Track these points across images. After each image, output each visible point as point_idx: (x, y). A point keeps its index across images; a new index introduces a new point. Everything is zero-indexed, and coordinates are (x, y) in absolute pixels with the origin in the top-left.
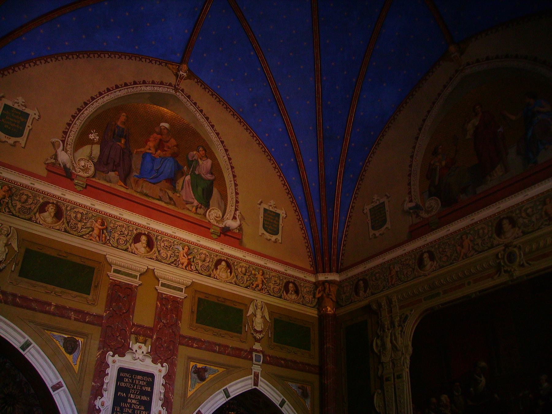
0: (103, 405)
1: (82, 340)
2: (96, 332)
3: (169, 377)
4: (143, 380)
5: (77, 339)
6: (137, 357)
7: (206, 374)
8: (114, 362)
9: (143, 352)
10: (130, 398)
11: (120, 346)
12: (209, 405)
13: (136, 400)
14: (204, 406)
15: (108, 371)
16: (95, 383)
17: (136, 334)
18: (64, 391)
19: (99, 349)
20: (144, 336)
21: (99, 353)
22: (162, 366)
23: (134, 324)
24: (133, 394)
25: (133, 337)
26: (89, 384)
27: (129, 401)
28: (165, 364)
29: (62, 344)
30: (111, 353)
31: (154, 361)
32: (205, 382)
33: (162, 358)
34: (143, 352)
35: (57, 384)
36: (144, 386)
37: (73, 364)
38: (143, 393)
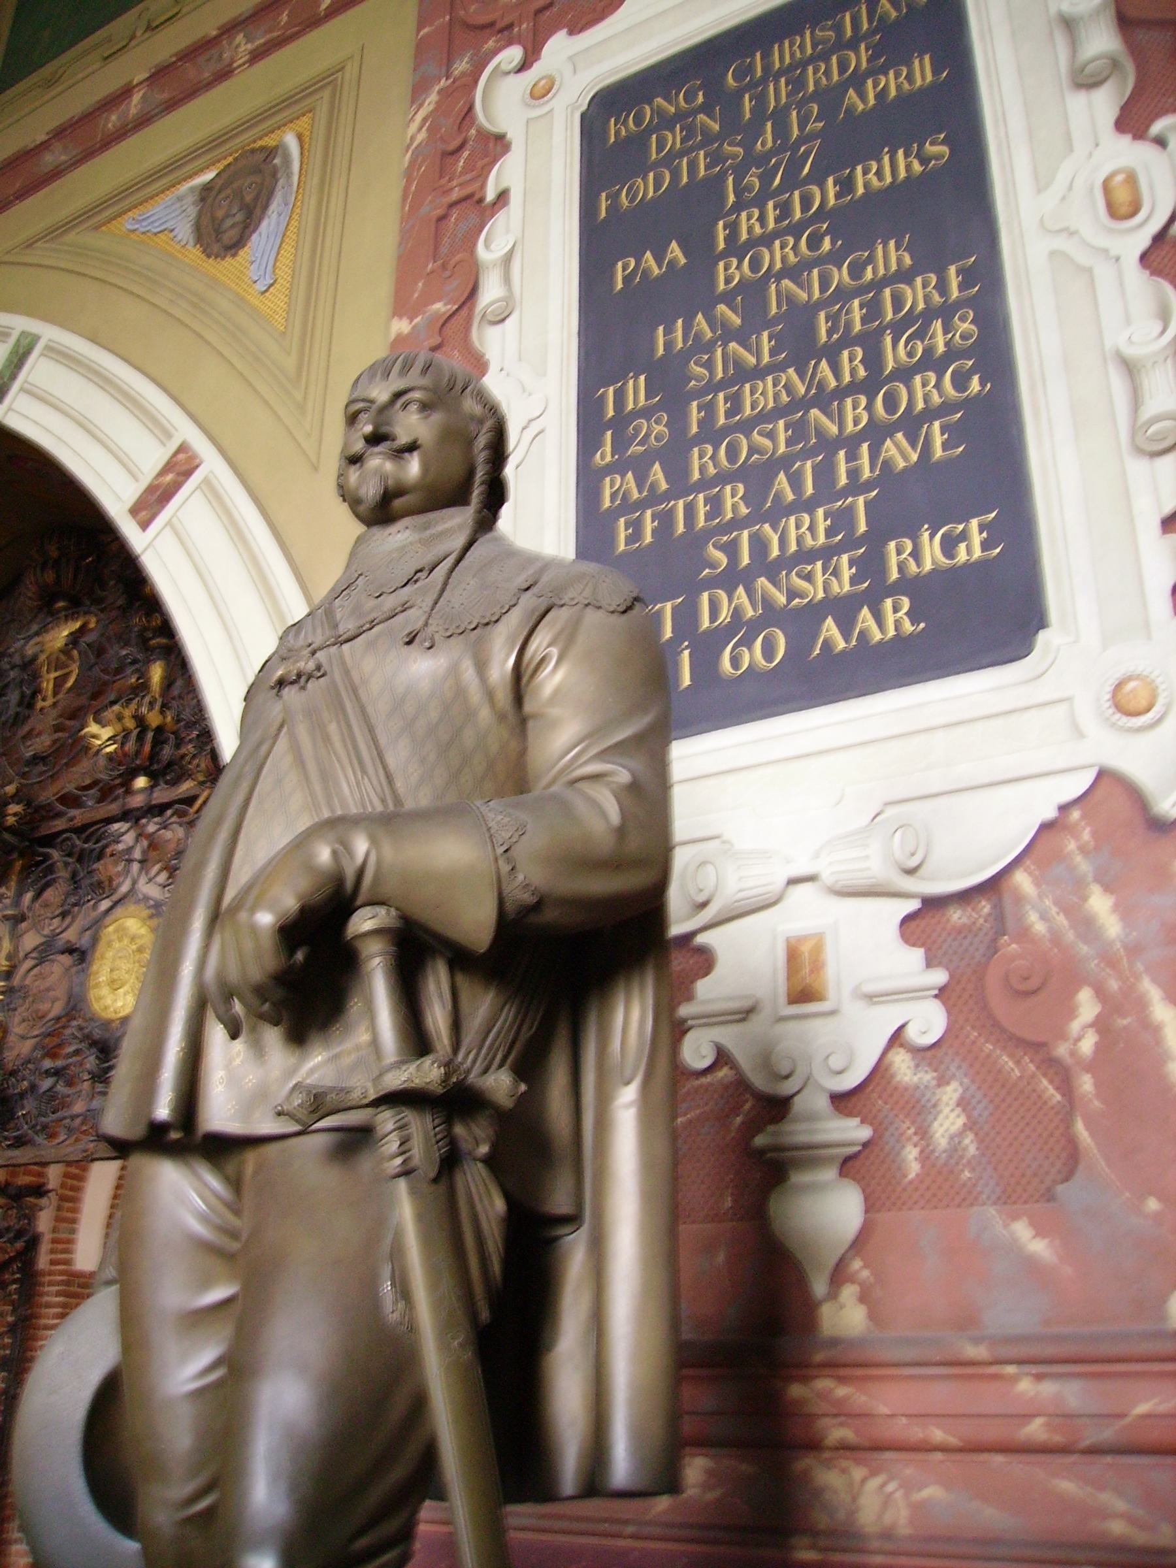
10: (735, 249)
13: (796, 231)
18: (210, 488)
36: (857, 81)
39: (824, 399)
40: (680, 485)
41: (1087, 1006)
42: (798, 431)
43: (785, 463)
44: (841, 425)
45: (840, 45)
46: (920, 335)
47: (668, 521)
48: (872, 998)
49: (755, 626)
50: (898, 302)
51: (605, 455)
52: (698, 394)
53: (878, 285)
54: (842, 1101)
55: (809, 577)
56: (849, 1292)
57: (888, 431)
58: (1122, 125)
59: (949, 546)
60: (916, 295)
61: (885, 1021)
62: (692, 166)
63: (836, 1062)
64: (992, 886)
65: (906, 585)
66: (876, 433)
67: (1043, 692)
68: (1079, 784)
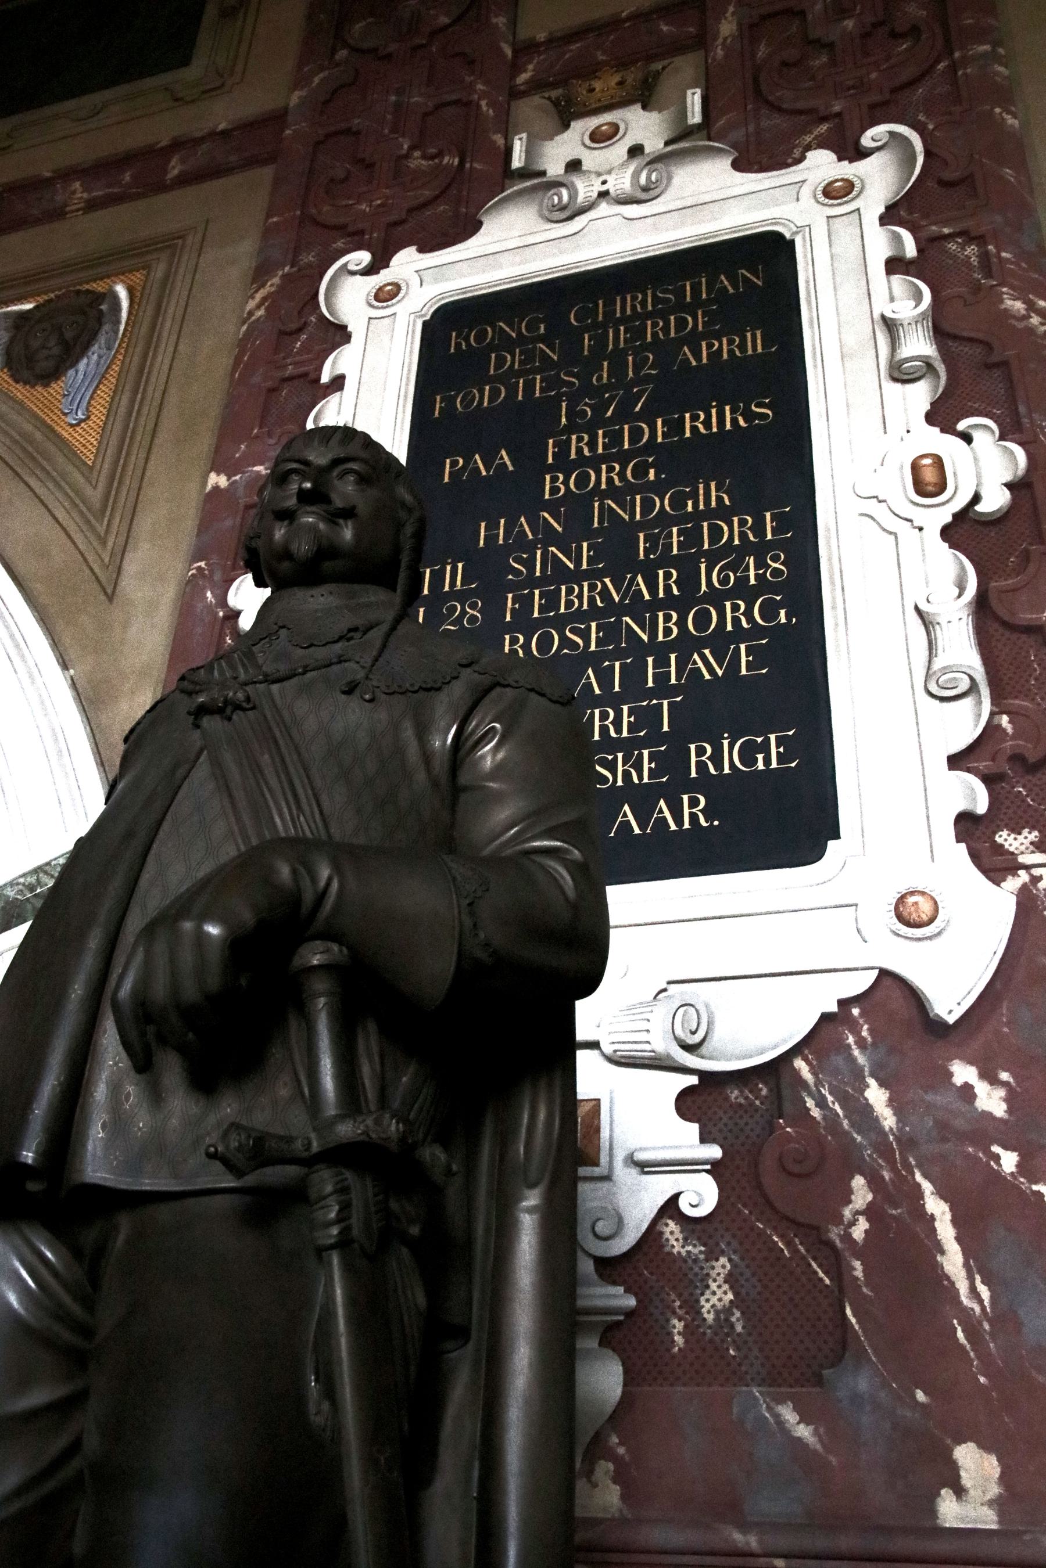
10: (563, 464)
13: (624, 458)
17: (562, 82)
20: (622, 65)
21: (259, 296)
23: (526, 49)
28: (873, 135)
33: (837, 108)
36: (693, 340)
39: (637, 608)
42: (610, 633)
43: (594, 660)
44: (653, 634)
45: (681, 306)
46: (733, 566)
48: (644, 1167)
50: (716, 533)
52: (513, 587)
53: (698, 516)
55: (612, 767)
56: (605, 1468)
57: (698, 645)
58: (931, 418)
59: (748, 755)
60: (732, 531)
62: (529, 387)
63: (601, 1227)
65: (705, 783)
66: (686, 645)
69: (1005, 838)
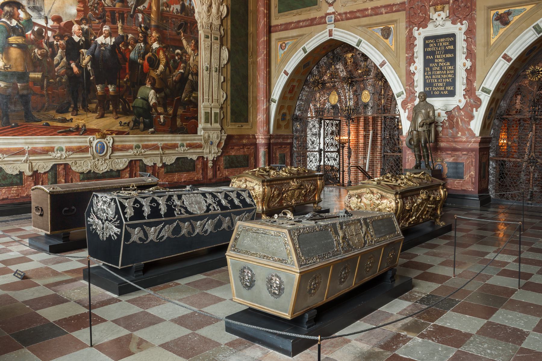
0: (416, 69)
1: (393, 25)
2: (401, 16)
3: (470, 33)
4: (446, 41)
5: (389, 26)
6: (437, 23)
7: (510, 17)
8: (419, 34)
9: (442, 18)
10: (437, 59)
11: (422, 20)
12: (517, 45)
13: (442, 58)
14: (510, 48)
15: (416, 42)
16: (408, 54)
17: (434, 5)
18: (387, 65)
19: (407, 28)
20: (441, 4)
22: (462, 24)
24: (439, 55)
25: (432, 9)
26: (403, 56)
27: (436, 61)
28: (464, 22)
29: (380, 34)
30: (416, 28)
31: (454, 23)
32: (509, 25)
34: (442, 18)
35: (382, 62)
36: (447, 46)
37: (390, 45)
38: (447, 52)
39: (443, 74)
40: (432, 78)
41: (455, 119)
42: (441, 76)
43: (440, 79)
47: (431, 81)
49: (437, 91)
51: (426, 74)
54: (441, 123)
60: (450, 68)
61: (444, 118)
64: (451, 111)
65: (447, 90)
66: (446, 78)
67: (455, 99)
68: (456, 106)
69: (466, 96)
